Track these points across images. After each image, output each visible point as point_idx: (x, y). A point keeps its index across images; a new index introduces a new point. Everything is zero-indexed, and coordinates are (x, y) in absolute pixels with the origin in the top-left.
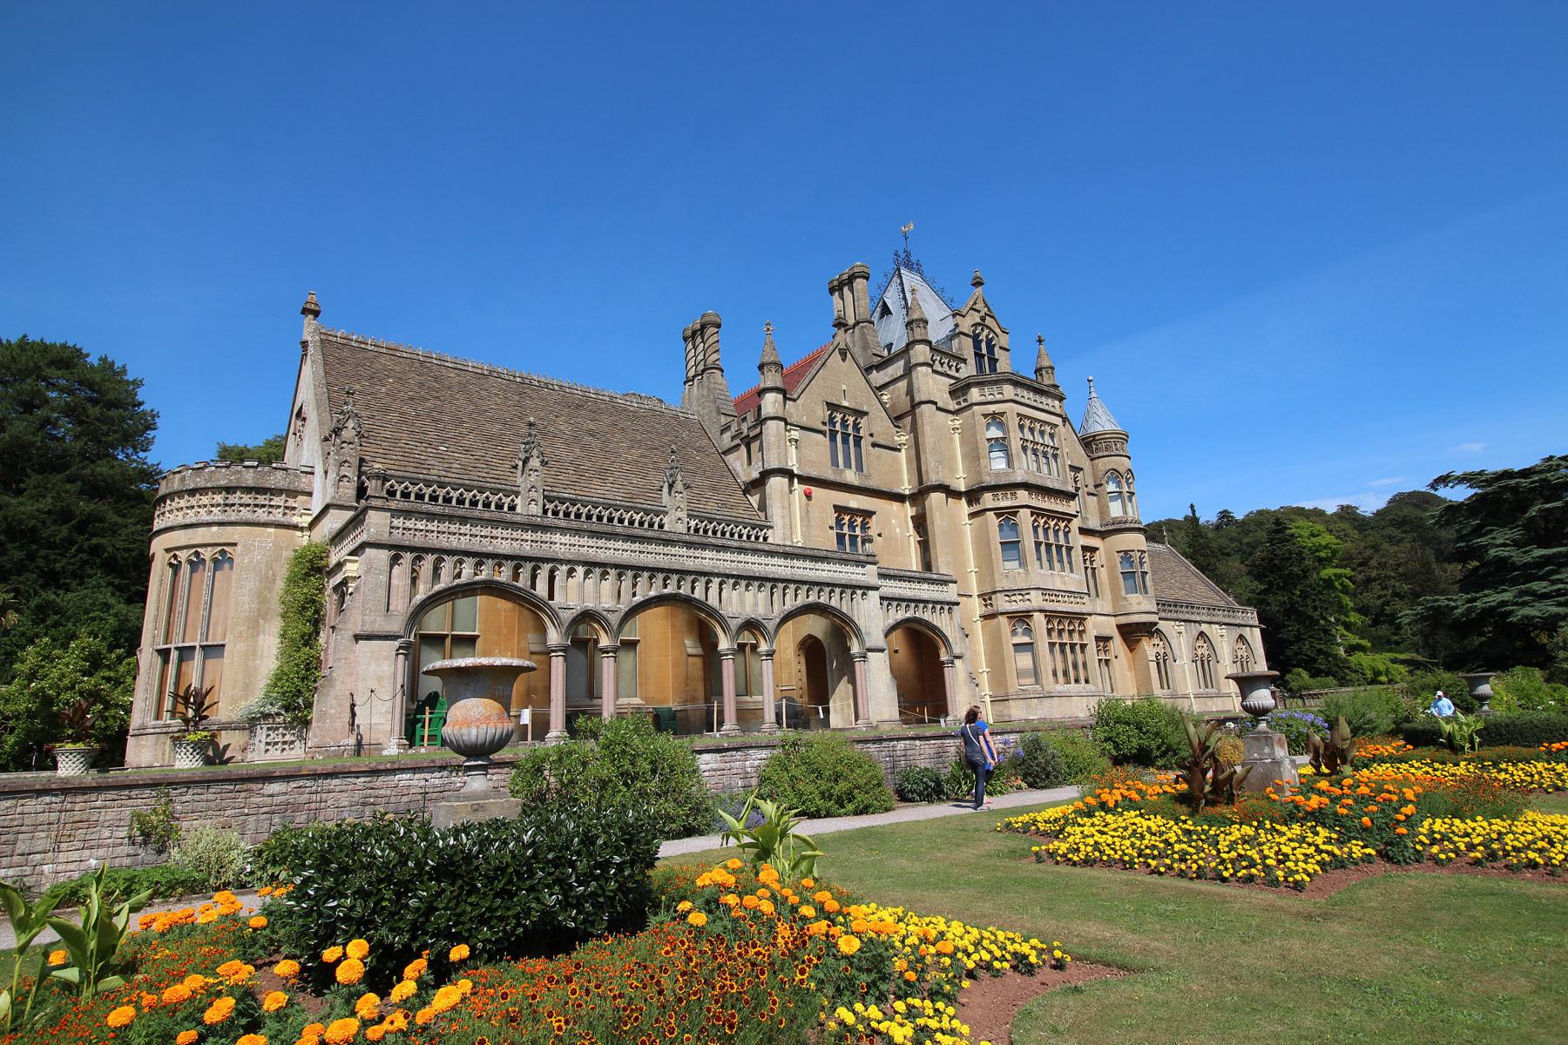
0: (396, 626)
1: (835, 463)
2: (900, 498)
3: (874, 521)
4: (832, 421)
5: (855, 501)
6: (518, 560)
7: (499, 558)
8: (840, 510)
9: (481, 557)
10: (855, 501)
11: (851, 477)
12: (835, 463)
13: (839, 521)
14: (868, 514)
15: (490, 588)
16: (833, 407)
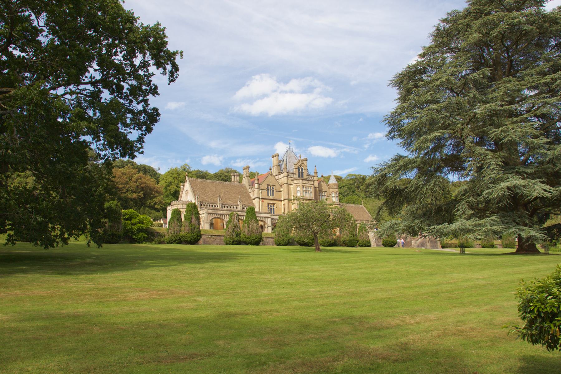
0: (209, 222)
1: (268, 195)
2: (281, 201)
3: (275, 205)
4: (268, 188)
5: (271, 202)
6: (221, 214)
7: (218, 214)
8: (269, 204)
9: (217, 214)
10: (271, 202)
11: (271, 197)
12: (268, 195)
13: (268, 206)
14: (274, 204)
15: (218, 218)
16: (268, 185)
